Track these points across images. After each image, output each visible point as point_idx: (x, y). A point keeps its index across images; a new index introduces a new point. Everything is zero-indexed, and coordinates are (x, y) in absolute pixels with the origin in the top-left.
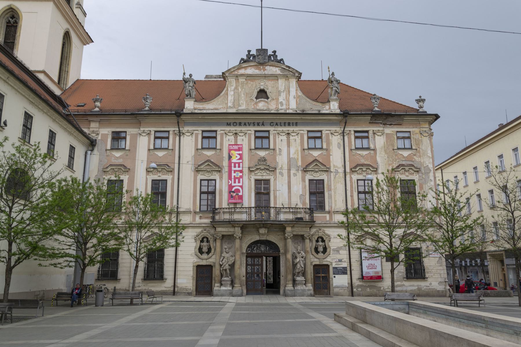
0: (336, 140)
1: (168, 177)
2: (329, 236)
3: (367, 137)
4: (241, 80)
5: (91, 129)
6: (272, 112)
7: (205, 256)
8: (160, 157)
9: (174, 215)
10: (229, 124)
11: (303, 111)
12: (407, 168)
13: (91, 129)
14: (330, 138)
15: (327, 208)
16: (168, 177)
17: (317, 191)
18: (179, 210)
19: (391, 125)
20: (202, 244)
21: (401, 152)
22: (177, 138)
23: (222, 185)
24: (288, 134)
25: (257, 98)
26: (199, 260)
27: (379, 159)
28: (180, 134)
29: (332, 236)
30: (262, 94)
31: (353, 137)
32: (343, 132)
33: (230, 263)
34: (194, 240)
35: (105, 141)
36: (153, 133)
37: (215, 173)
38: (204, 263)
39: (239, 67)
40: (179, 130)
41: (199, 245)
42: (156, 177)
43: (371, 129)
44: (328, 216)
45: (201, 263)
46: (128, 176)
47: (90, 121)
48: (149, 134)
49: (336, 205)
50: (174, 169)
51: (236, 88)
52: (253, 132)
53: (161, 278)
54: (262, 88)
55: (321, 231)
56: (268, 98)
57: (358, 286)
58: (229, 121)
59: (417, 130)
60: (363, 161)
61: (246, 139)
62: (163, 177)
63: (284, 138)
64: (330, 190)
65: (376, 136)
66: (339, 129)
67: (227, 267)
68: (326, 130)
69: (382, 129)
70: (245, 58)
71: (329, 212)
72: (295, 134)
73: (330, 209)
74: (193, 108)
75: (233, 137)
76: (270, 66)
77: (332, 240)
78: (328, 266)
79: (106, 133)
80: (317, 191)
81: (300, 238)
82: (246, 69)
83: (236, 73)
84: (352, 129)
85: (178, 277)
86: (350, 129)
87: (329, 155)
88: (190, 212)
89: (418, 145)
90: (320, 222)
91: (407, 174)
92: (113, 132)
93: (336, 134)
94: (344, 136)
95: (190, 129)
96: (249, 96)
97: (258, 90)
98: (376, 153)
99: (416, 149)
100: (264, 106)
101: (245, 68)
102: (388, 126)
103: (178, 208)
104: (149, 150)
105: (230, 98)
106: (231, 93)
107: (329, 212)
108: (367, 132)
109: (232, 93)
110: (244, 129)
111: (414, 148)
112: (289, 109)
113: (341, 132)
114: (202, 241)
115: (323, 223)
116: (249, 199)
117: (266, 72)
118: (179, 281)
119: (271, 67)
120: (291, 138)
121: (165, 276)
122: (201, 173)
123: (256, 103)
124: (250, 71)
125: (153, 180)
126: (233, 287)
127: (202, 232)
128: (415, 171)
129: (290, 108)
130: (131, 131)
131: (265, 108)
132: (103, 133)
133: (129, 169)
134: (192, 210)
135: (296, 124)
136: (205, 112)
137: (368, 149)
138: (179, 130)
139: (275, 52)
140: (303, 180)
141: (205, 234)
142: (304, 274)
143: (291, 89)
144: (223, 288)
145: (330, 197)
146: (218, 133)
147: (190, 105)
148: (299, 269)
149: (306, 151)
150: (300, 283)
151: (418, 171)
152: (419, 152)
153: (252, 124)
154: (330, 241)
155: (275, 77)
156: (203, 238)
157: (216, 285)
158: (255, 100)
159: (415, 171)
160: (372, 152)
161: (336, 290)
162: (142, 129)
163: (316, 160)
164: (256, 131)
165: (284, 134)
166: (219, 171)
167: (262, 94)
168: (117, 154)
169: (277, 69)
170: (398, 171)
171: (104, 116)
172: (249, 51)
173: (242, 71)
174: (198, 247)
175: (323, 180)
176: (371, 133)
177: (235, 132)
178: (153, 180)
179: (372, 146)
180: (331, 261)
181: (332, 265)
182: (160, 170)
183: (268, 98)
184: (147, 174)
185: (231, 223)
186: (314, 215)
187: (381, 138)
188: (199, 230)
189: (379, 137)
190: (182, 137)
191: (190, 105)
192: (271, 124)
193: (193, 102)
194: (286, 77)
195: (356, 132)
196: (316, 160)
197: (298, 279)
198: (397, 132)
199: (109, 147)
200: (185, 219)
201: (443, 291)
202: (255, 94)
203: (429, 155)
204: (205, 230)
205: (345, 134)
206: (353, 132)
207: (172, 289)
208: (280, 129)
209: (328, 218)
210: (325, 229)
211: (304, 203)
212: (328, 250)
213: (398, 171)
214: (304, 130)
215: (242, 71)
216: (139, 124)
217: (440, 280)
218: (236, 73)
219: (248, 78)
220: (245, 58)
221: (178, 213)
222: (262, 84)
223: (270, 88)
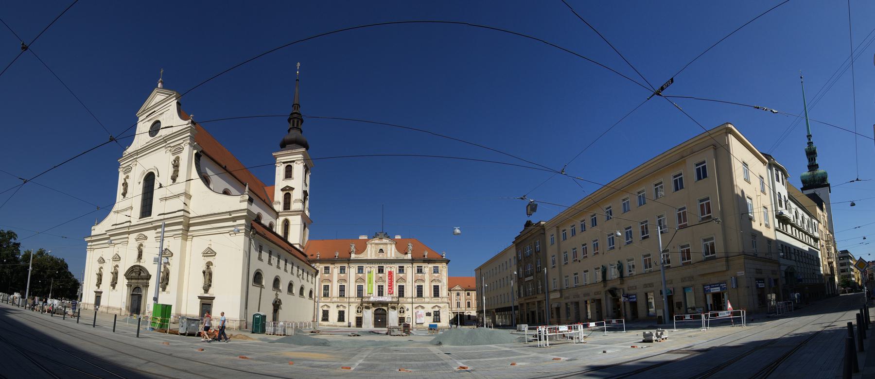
23: (365, 287)
30: (381, 251)
53: (343, 321)
61: (375, 268)
68: (405, 266)
80: (401, 290)
81: (394, 308)
86: (415, 265)
105: (369, 252)
116: (375, 291)
130: (331, 266)
132: (321, 267)
147: (353, 256)
167: (381, 251)
168: (327, 275)
171: (321, 261)
185: (368, 303)
187: (428, 268)
191: (353, 256)
200: (352, 300)
222: (381, 247)
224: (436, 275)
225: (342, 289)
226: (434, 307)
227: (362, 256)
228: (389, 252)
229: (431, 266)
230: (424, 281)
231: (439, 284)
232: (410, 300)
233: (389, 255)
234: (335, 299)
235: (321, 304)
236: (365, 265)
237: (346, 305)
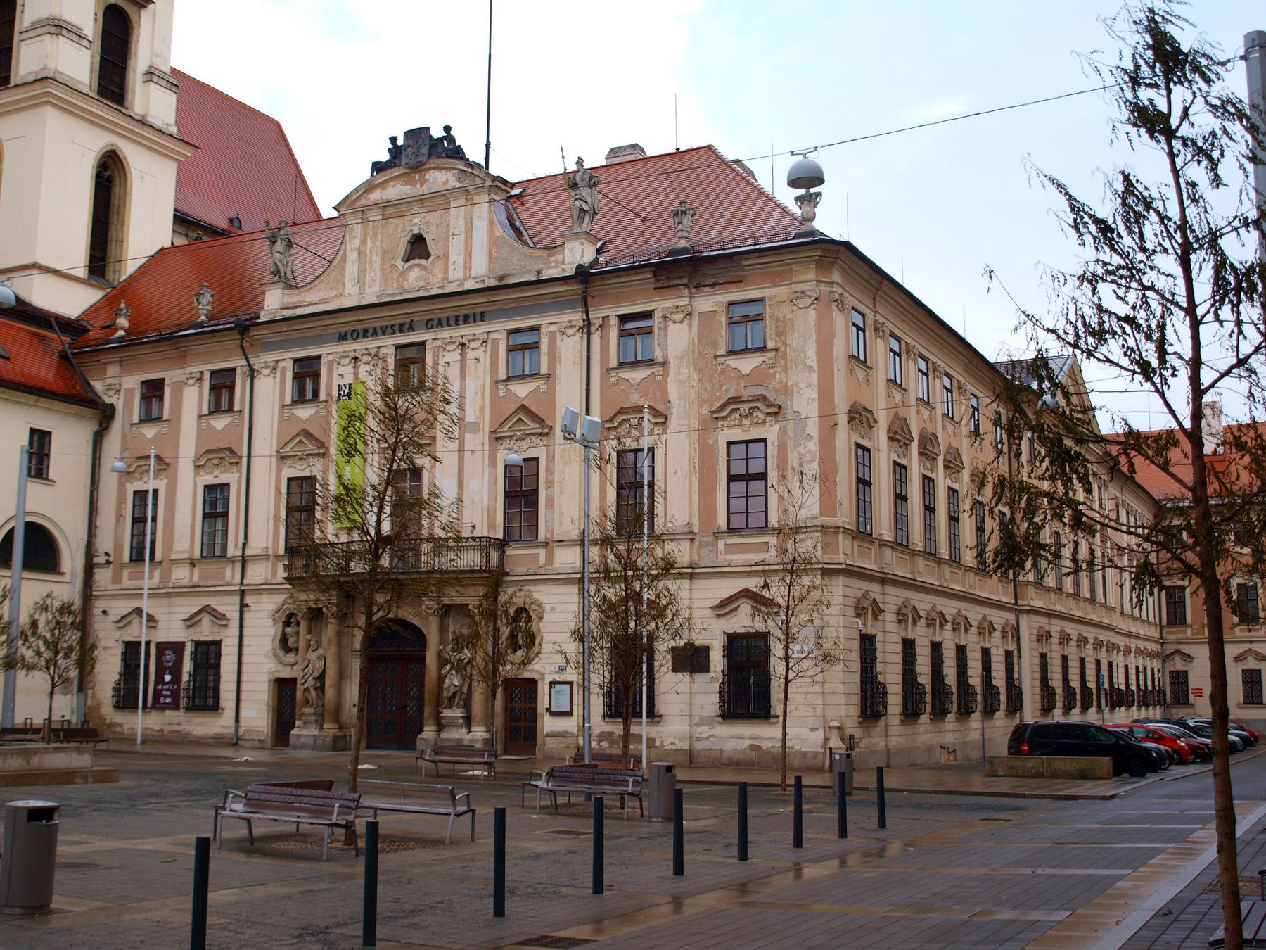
0: (571, 347)
1: (231, 477)
2: (540, 606)
3: (648, 331)
4: (374, 216)
5: (108, 382)
6: (434, 292)
7: (290, 658)
8: (220, 432)
9: (238, 567)
10: (343, 337)
11: (502, 278)
12: (744, 408)
13: (108, 382)
14: (559, 343)
15: (542, 535)
16: (231, 477)
17: (521, 493)
18: (249, 552)
19: (714, 285)
20: (288, 630)
21: (734, 362)
22: (248, 383)
24: (463, 345)
25: (407, 259)
26: (280, 667)
27: (673, 391)
28: (252, 373)
29: (547, 607)
31: (613, 334)
32: (587, 326)
33: (317, 674)
34: (270, 622)
35: (128, 405)
36: (207, 376)
37: (312, 460)
38: (286, 673)
39: (367, 188)
40: (249, 365)
41: (279, 633)
42: (211, 480)
43: (660, 305)
44: (542, 552)
45: (283, 675)
46: (165, 481)
47: (105, 364)
48: (200, 379)
49: (561, 525)
50: (241, 458)
51: (364, 242)
52: (392, 350)
54: (416, 231)
55: (522, 594)
56: (426, 255)
57: (603, 736)
58: (342, 330)
59: (780, 291)
60: (634, 399)
62: (223, 478)
63: (454, 357)
64: (550, 485)
65: (670, 323)
66: (577, 317)
67: (310, 683)
68: (548, 322)
69: (685, 301)
70: (385, 157)
71: (546, 544)
72: (478, 343)
73: (549, 536)
74: (277, 306)
75: (350, 369)
76: (434, 168)
77: (546, 617)
78: (533, 683)
79: (132, 385)
80: (521, 493)
82: (384, 189)
83: (363, 202)
84: (613, 312)
85: (243, 705)
87: (552, 393)
88: (267, 557)
89: (781, 334)
90: (524, 570)
91: (746, 422)
92: (143, 382)
93: (570, 331)
94: (589, 334)
95: (269, 357)
96: (390, 256)
97: (408, 238)
98: (666, 374)
99: (777, 350)
100: (418, 279)
101: (382, 185)
102: (707, 289)
103: (244, 545)
104: (200, 417)
106: (352, 256)
107: (546, 544)
108: (648, 315)
109: (354, 255)
110: (371, 344)
111: (770, 345)
112: (466, 278)
113: (581, 323)
114: (287, 623)
115: (531, 571)
117: (425, 189)
118: (244, 713)
119: (437, 173)
120: (471, 355)
121: (223, 703)
122: (289, 462)
123: (404, 274)
124: (395, 191)
125: (206, 487)
126: (321, 728)
127: (284, 603)
128: (768, 414)
129: (473, 275)
130: (171, 376)
131: (421, 284)
133: (168, 465)
134: (270, 552)
135: (482, 317)
136: (299, 312)
137: (649, 362)
138: (249, 365)
139: (447, 129)
140: (493, 463)
141: (290, 607)
142: (467, 704)
143: (476, 223)
144: (305, 732)
145: (550, 502)
146: (323, 360)
147: (274, 301)
148: (448, 688)
149: (501, 386)
150: (453, 724)
151: (777, 411)
152: (784, 357)
153: (389, 330)
154: (541, 618)
155: (439, 200)
156: (290, 616)
157: (297, 723)
158: (400, 264)
159: (768, 414)
160: (658, 370)
161: (551, 743)
162: (188, 370)
163: (523, 406)
164: (398, 347)
165: (454, 347)
166: (323, 455)
167: (418, 247)
168: (150, 431)
169: (450, 174)
170: (724, 418)
172: (393, 140)
173: (376, 196)
174: (278, 638)
175: (537, 459)
176: (657, 315)
177: (354, 354)
178: (206, 487)
179: (658, 355)
180: (542, 670)
181: (543, 679)
182: (216, 461)
183: (426, 255)
184: (196, 474)
186: (508, 553)
188: (280, 598)
189: (678, 325)
190: (256, 380)
192: (429, 325)
193: (280, 291)
194: (465, 193)
195: (623, 319)
196: (524, 409)
197: (447, 713)
198: (730, 304)
199: (136, 419)
201: (815, 754)
202: (402, 248)
203: (809, 362)
204: (291, 597)
205: (593, 329)
206: (614, 321)
207: (232, 730)
208: (446, 333)
209: (542, 560)
210: (533, 588)
211: (492, 525)
212: (537, 642)
213: (724, 418)
214: (498, 329)
215: (376, 196)
216: (181, 359)
217: (811, 722)
218: (363, 202)
219: (388, 211)
220: (385, 157)
221: (244, 561)
222: (415, 223)
223: (433, 228)
224: (746, 364)
225: (215, 504)
226: (725, 607)
227: (315, 299)
228: (456, 256)
229: (711, 302)
230: (662, 419)
231: (771, 432)
232: (568, 559)
233: (456, 273)
234: (181, 575)
235: (120, 607)
236: (327, 352)
237: (229, 607)
